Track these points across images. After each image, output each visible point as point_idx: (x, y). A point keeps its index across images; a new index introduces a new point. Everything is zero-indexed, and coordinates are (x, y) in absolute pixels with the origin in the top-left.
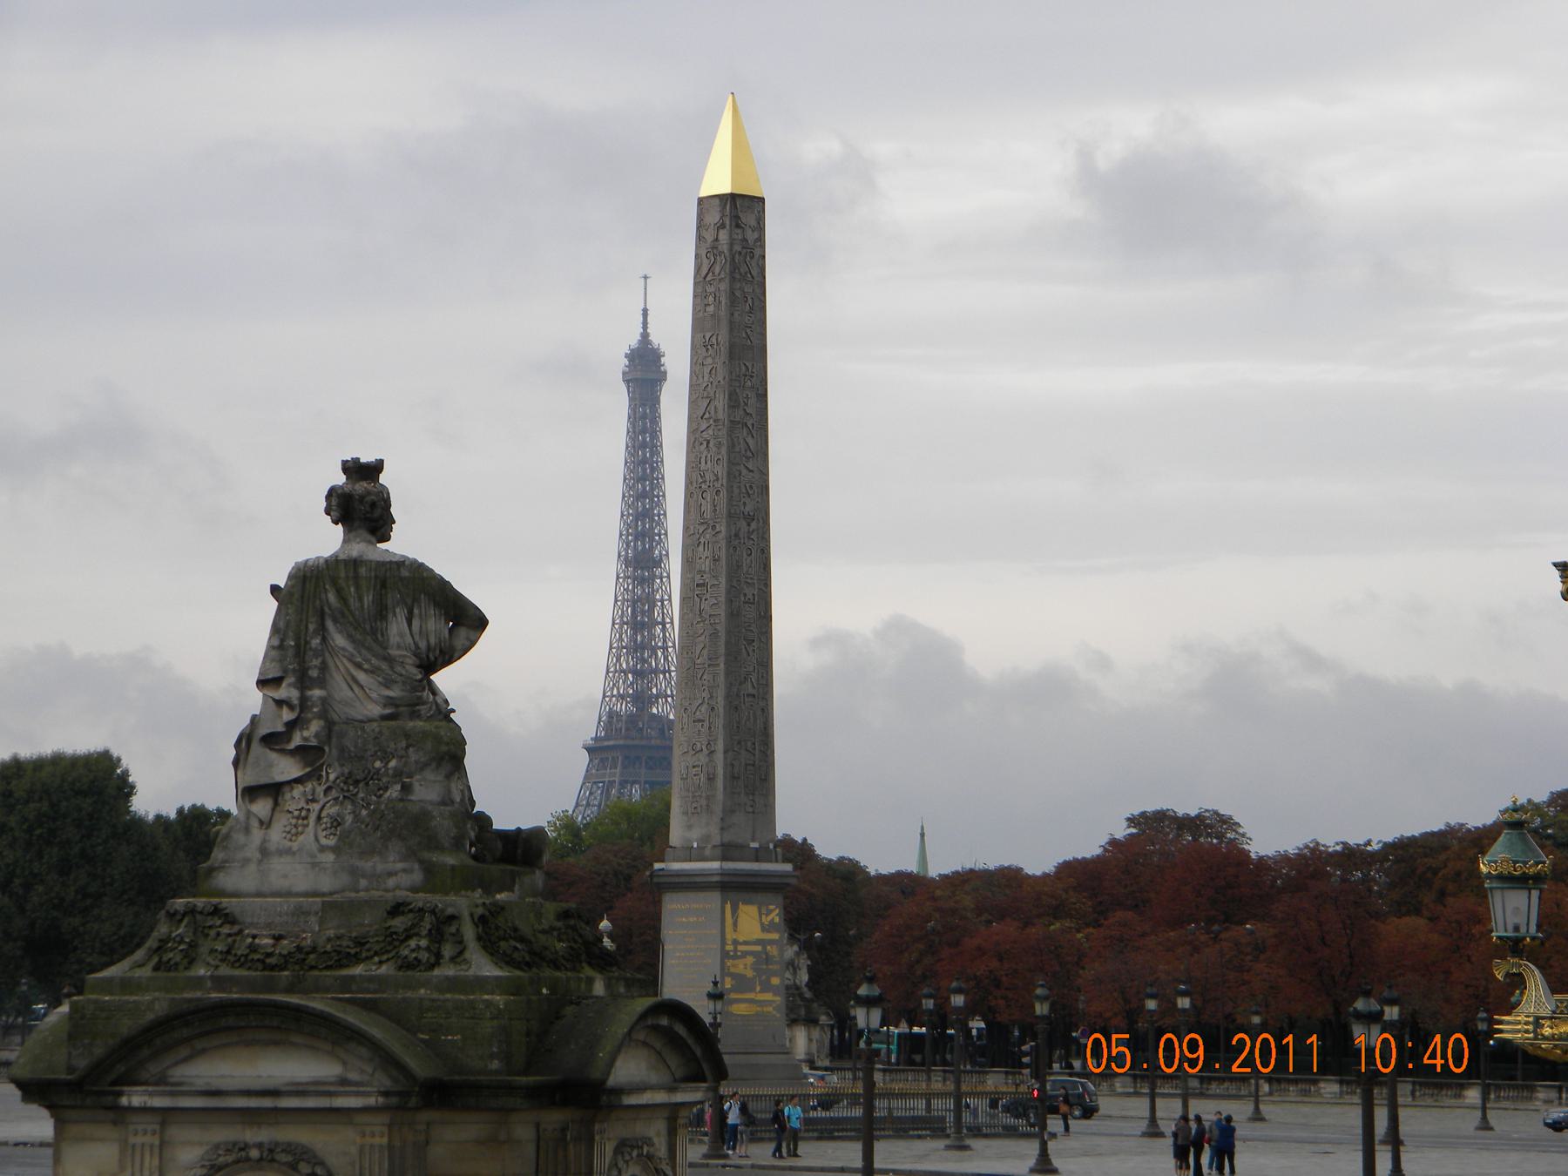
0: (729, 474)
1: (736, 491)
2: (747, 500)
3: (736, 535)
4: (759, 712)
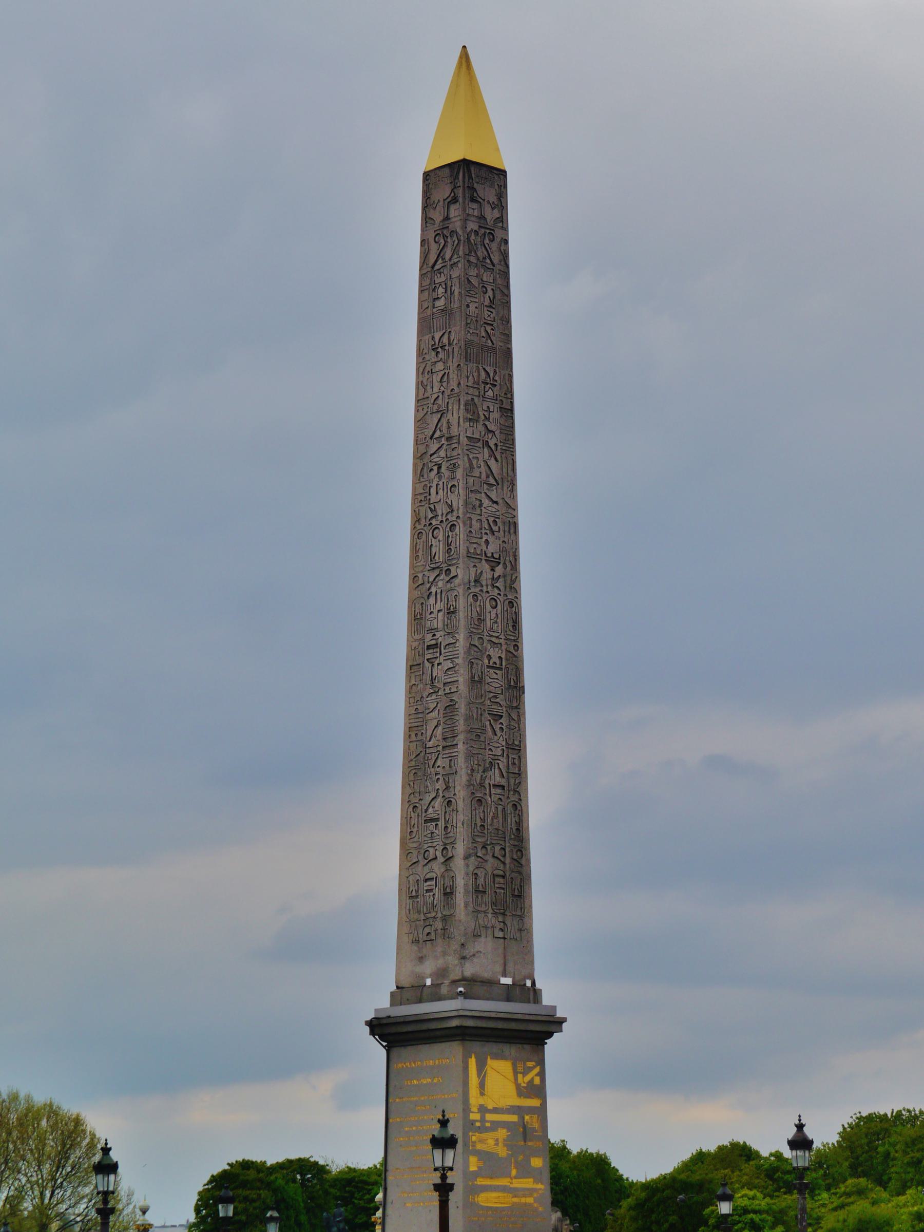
0: (466, 503)
1: (476, 525)
2: (491, 539)
3: (476, 581)
4: (509, 809)
